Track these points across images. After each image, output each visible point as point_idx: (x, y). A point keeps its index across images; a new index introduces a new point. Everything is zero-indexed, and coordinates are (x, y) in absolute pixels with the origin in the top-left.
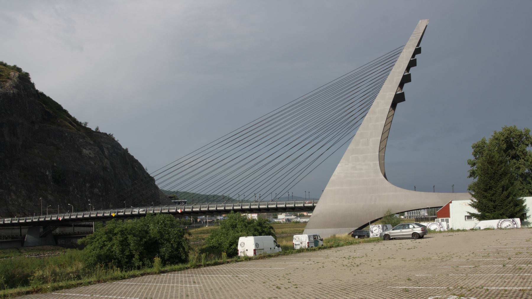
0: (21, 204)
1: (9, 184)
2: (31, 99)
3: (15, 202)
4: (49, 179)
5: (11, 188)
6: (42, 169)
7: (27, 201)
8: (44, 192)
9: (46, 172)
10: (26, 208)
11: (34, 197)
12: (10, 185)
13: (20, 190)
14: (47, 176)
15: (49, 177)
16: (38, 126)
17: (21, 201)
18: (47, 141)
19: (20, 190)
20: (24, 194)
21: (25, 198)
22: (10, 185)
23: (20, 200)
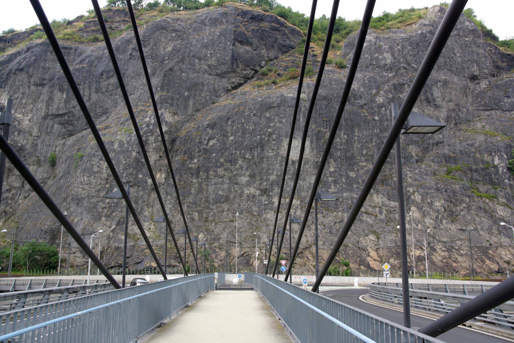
0: (428, 228)
1: (408, 189)
2: (467, 39)
3: (417, 225)
4: (500, 172)
5: (412, 197)
6: (486, 155)
7: (444, 221)
8: (487, 201)
9: (493, 161)
10: (437, 238)
11: (462, 213)
12: (411, 191)
13: (429, 201)
14: (495, 167)
15: (501, 170)
16: (487, 83)
17: (431, 221)
18: (502, 103)
19: (429, 201)
20: (439, 208)
21: (440, 216)
22: (411, 191)
23: (428, 221)
